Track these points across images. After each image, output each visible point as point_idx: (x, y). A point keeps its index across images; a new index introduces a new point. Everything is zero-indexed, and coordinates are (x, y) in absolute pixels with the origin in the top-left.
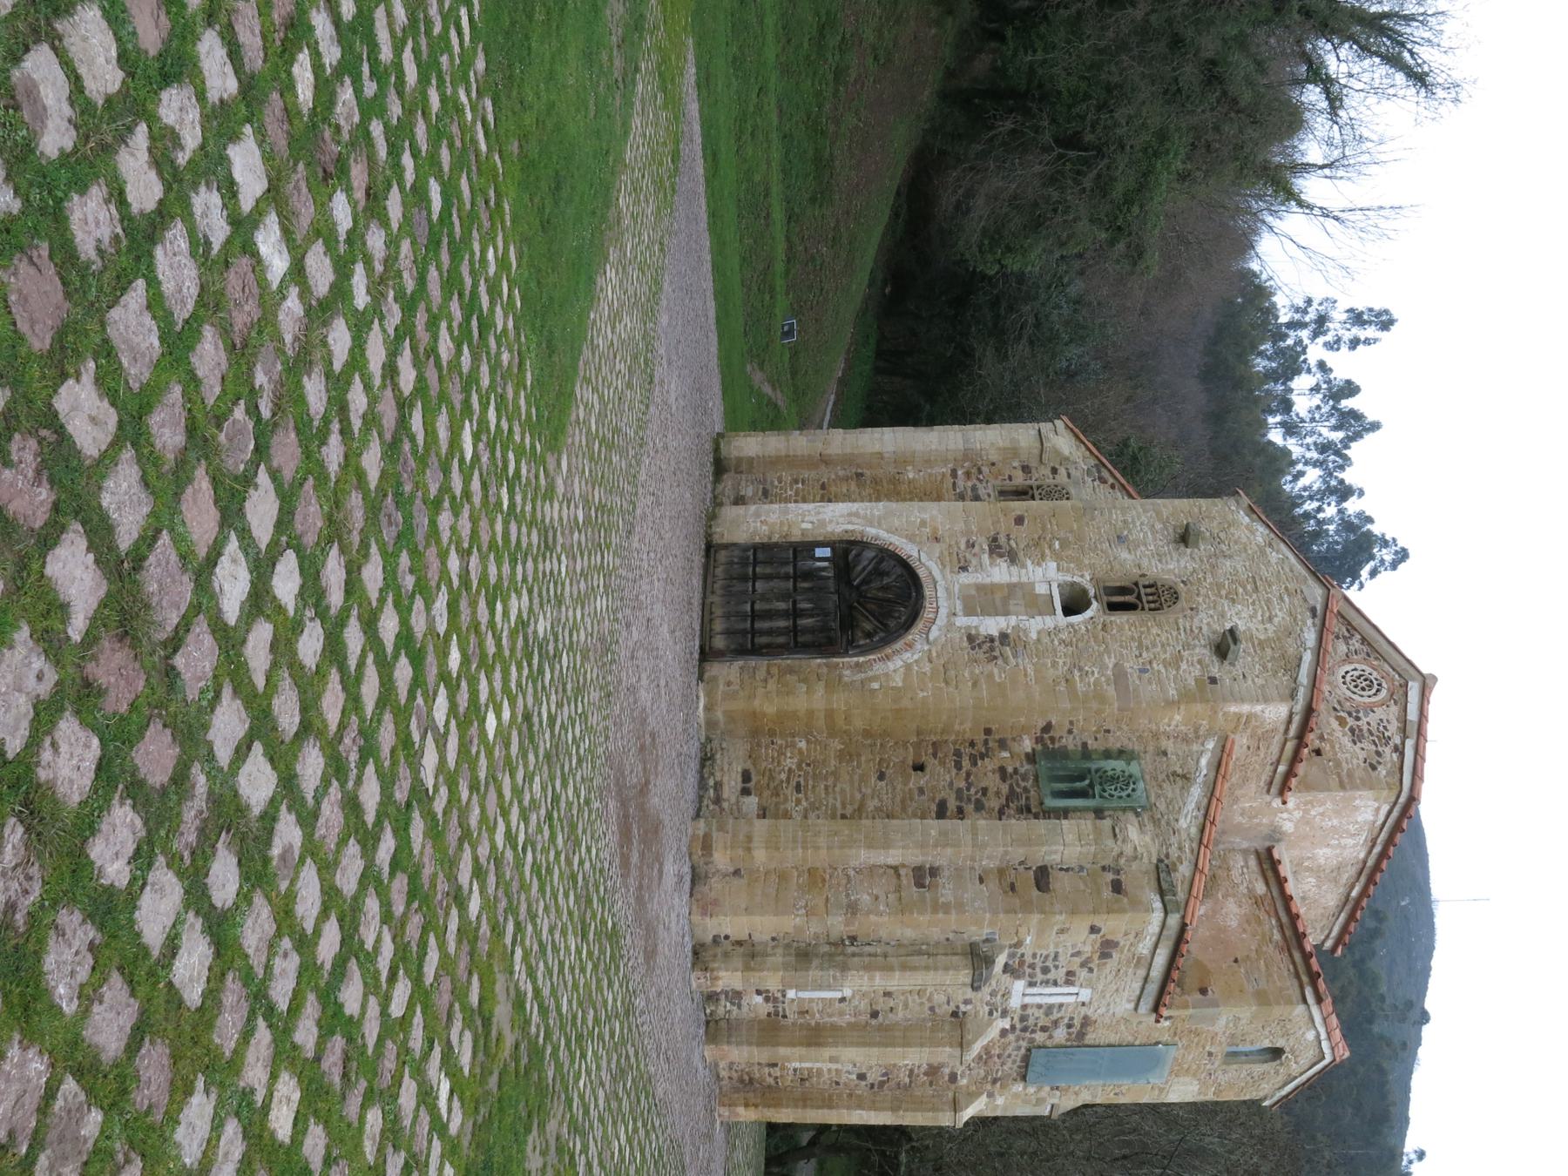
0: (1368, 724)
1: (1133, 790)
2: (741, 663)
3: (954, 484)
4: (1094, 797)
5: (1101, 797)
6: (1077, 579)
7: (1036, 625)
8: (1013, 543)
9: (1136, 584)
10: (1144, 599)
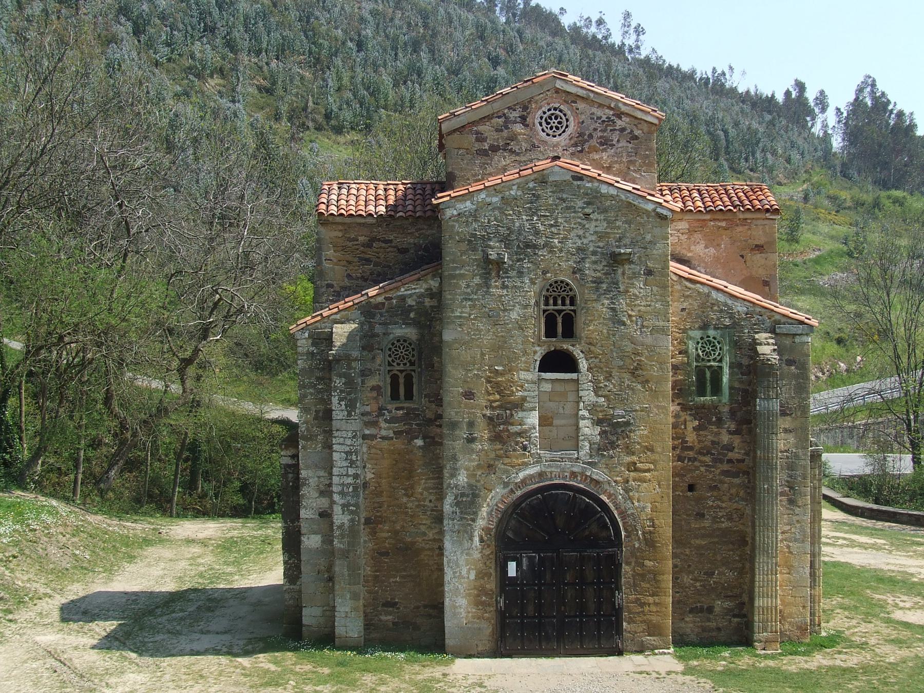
0: (595, 129)
1: (714, 338)
2: (624, 624)
3: (383, 438)
4: (721, 368)
5: (720, 361)
6: (538, 357)
7: (588, 395)
8: (495, 405)
9: (544, 311)
10: (560, 307)
